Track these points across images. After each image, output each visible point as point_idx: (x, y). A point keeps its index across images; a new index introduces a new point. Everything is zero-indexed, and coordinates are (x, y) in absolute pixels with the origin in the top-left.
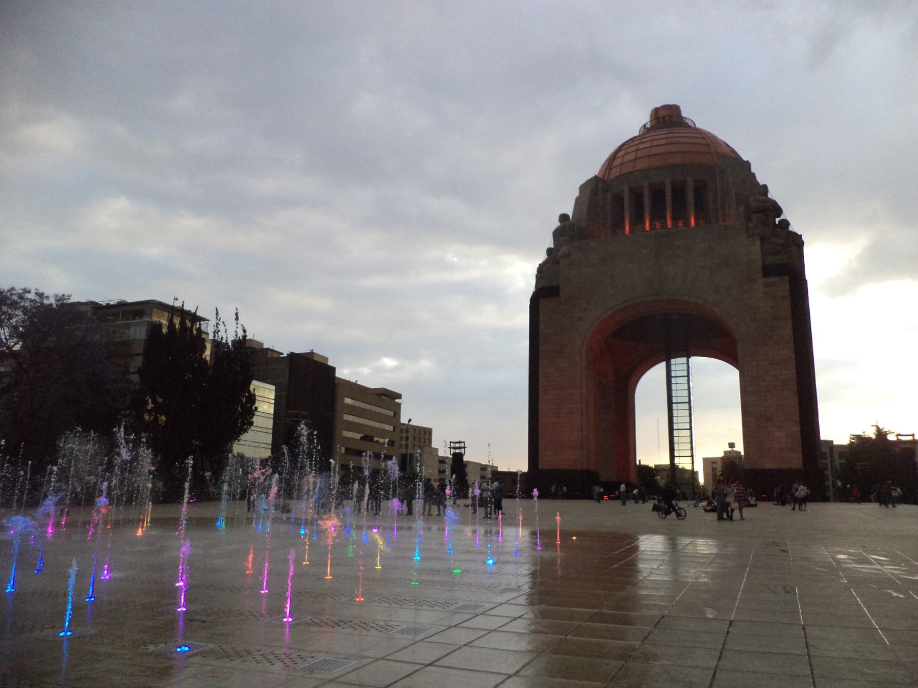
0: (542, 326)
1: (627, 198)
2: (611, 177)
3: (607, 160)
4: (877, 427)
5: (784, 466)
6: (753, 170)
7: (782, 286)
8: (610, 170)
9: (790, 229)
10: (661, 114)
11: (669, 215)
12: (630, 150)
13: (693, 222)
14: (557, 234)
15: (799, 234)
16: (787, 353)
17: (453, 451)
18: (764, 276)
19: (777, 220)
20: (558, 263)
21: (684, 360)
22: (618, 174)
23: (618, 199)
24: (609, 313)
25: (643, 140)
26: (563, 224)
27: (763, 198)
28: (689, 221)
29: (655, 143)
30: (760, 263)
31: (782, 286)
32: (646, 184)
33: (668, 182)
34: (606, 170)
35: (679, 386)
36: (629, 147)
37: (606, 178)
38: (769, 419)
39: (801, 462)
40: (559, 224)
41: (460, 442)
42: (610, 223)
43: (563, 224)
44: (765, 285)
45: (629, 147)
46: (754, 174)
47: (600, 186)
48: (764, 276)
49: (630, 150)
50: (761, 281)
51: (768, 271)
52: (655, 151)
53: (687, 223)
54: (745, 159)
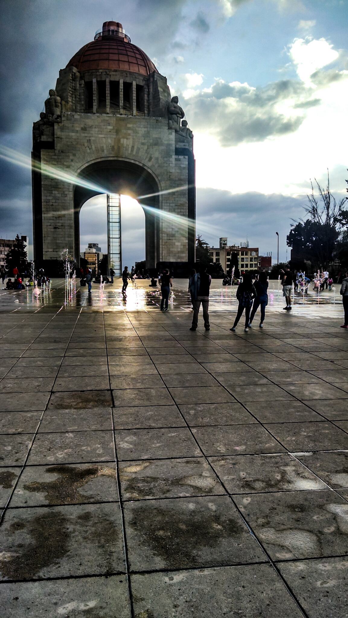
5: (179, 261)
9: (187, 127)
19: (182, 120)
25: (103, 47)
27: (175, 105)
30: (174, 146)
31: (185, 162)
33: (121, 82)
39: (187, 258)
42: (83, 102)
44: (176, 160)
50: (174, 157)
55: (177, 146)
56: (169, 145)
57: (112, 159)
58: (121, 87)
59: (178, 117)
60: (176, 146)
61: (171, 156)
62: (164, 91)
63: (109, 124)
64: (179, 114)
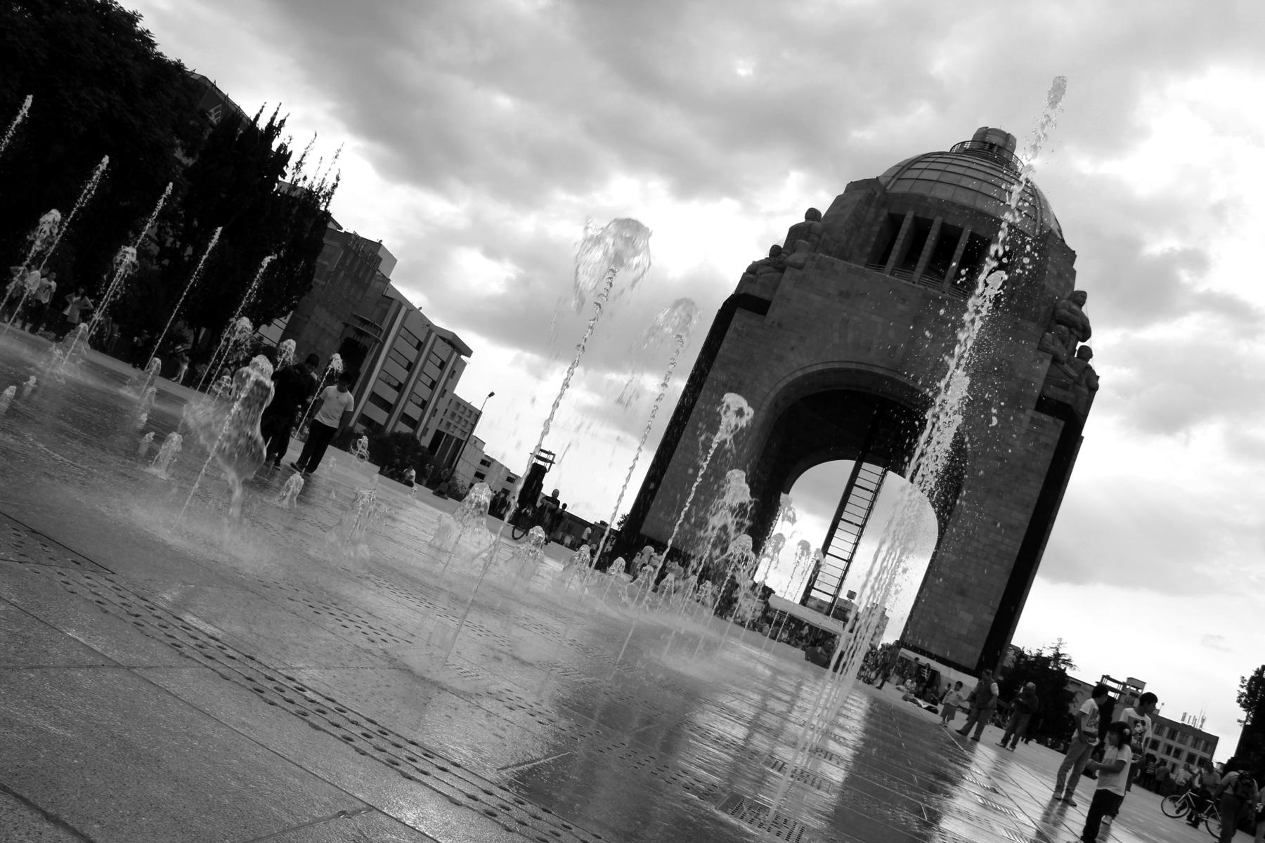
0: (725, 345)
1: (906, 226)
2: (896, 190)
3: (898, 166)
6: (1075, 267)
7: (1053, 428)
9: (1090, 362)
14: (795, 232)
15: (1098, 374)
16: (1022, 519)
17: (535, 460)
19: (1080, 344)
20: (782, 270)
21: (879, 470)
23: (894, 222)
24: (820, 367)
26: (810, 222)
27: (1075, 307)
29: (969, 172)
31: (1053, 428)
32: (938, 221)
33: (968, 231)
34: (894, 177)
35: (859, 499)
36: (933, 162)
37: (888, 188)
38: (962, 593)
41: (549, 453)
42: (869, 250)
44: (1033, 421)
45: (933, 162)
46: (1073, 273)
50: (1030, 412)
51: (1044, 405)
55: (1048, 393)
56: (1026, 383)
57: (881, 372)
59: (1071, 333)
60: (1042, 391)
61: (1024, 410)
62: (1060, 276)
63: (904, 300)
64: (1076, 328)
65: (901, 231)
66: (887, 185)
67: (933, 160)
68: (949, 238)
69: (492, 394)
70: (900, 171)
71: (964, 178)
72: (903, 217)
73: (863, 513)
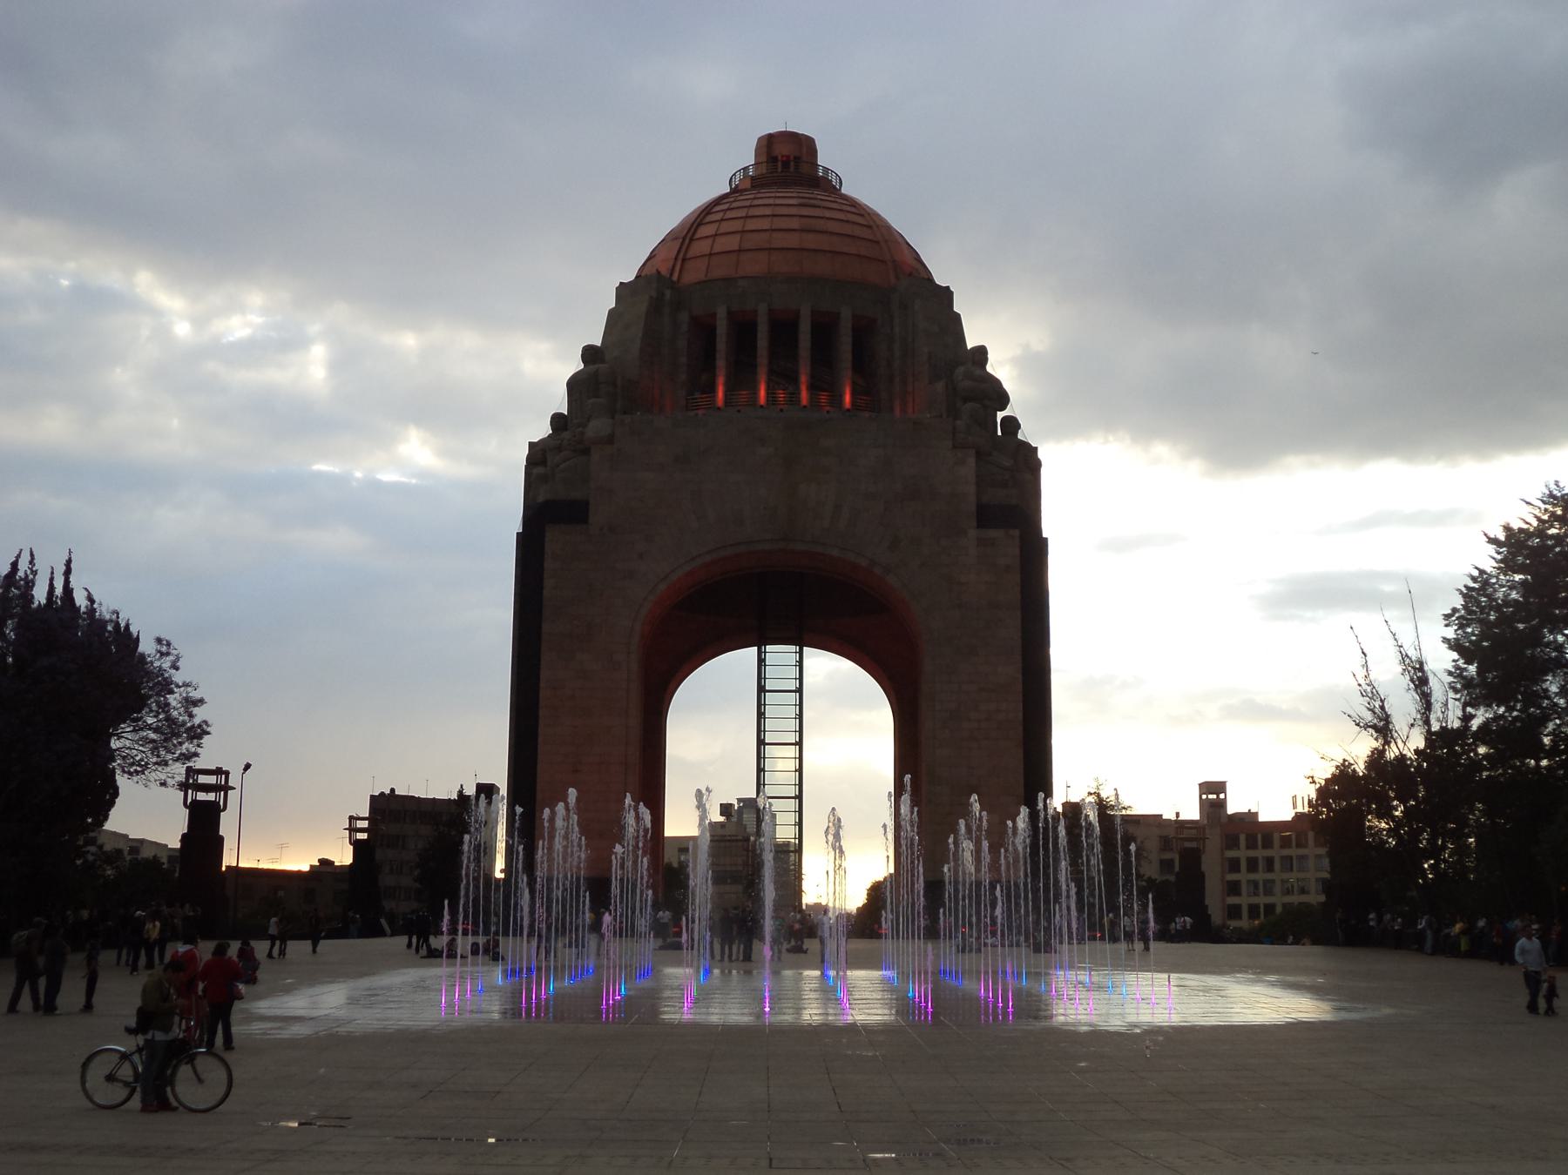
0: (548, 582)
4: (1098, 795)
8: (684, 260)
10: (782, 150)
11: (804, 379)
12: (725, 227)
13: (847, 399)
18: (978, 527)
19: (1000, 415)
20: (586, 452)
22: (702, 277)
23: (704, 330)
26: (593, 368)
27: (978, 372)
28: (841, 396)
32: (763, 309)
34: (676, 259)
35: (780, 709)
37: (675, 278)
40: (582, 366)
43: (593, 368)
46: (958, 317)
47: (668, 293)
48: (978, 527)
49: (725, 227)
50: (973, 533)
52: (780, 240)
53: (836, 400)
54: (940, 280)
58: (805, 328)
65: (718, 340)
66: (671, 274)
67: (718, 216)
68: (784, 328)
69: (247, 767)
70: (682, 244)
71: (775, 235)
72: (714, 315)
73: (793, 724)
